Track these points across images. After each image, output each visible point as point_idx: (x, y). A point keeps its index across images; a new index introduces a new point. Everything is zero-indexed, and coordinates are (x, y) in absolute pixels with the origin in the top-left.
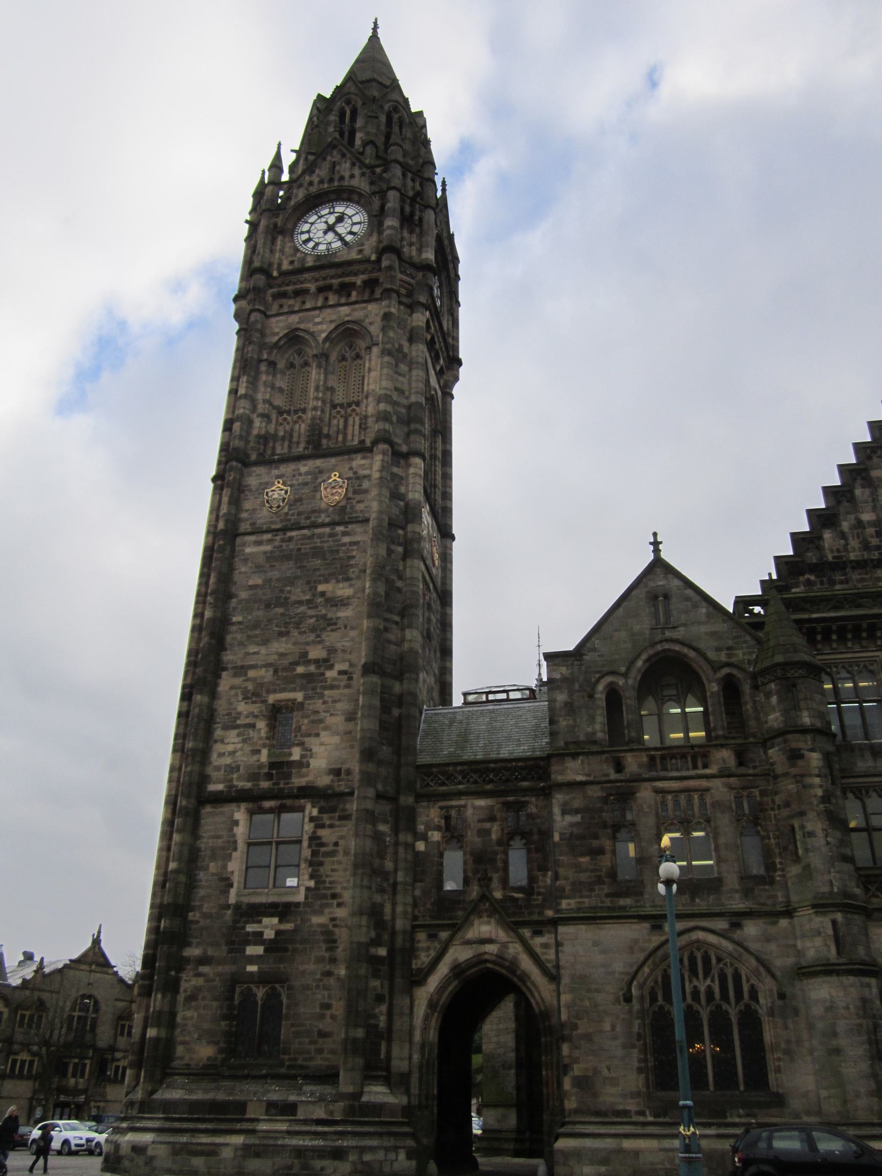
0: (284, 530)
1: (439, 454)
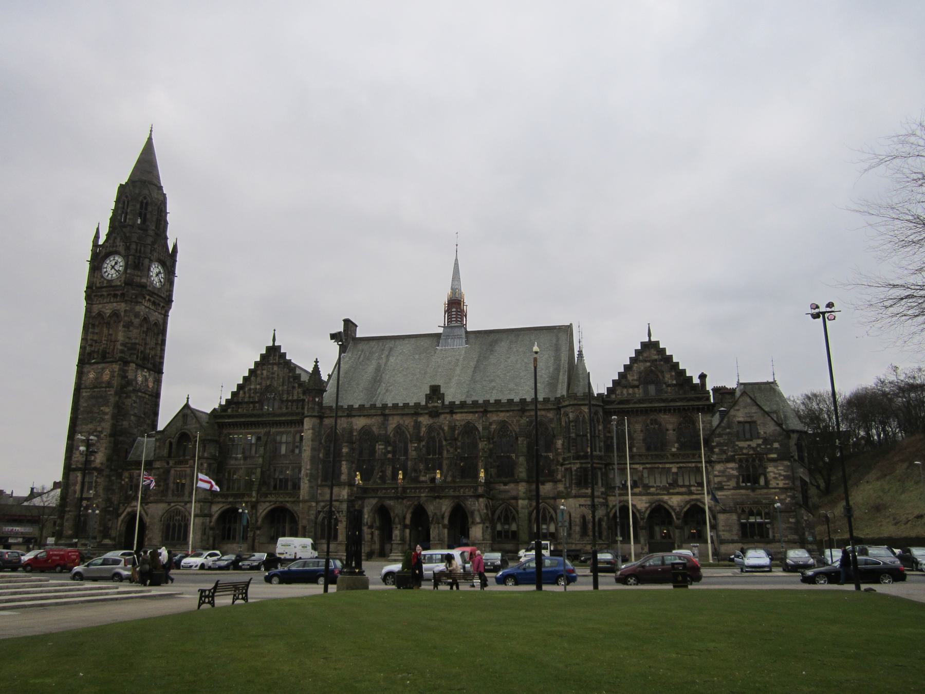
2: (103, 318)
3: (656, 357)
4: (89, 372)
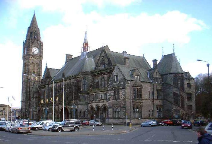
3: (104, 55)
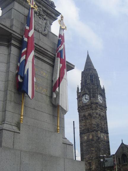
0: (87, 142)
1: (105, 122)
2: (85, 117)
4: (84, 137)
